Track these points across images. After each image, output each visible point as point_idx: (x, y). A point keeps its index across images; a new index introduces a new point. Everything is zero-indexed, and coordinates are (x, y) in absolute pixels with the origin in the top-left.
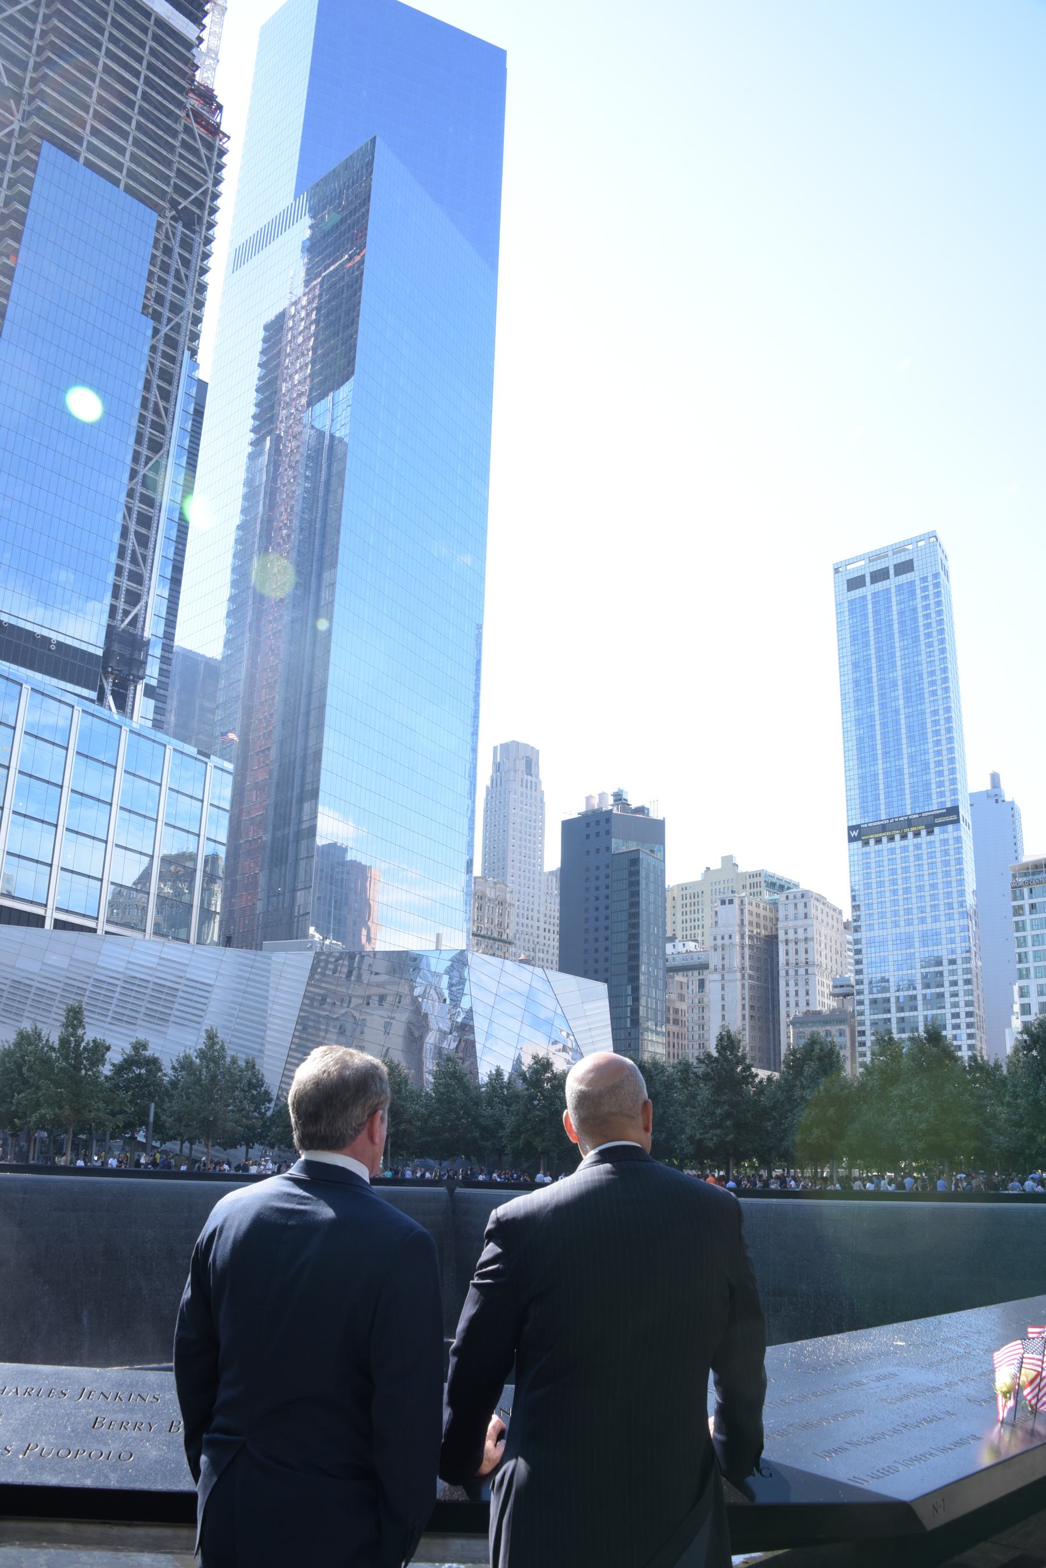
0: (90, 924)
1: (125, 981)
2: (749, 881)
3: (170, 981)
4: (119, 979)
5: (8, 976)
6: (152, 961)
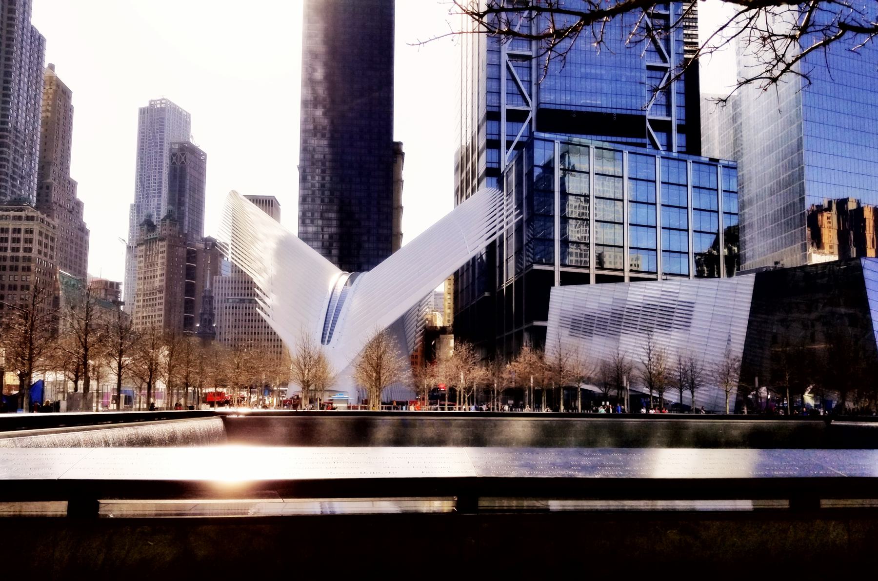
0: (654, 277)
3: (670, 304)
4: (640, 306)
5: (583, 312)
6: (657, 294)
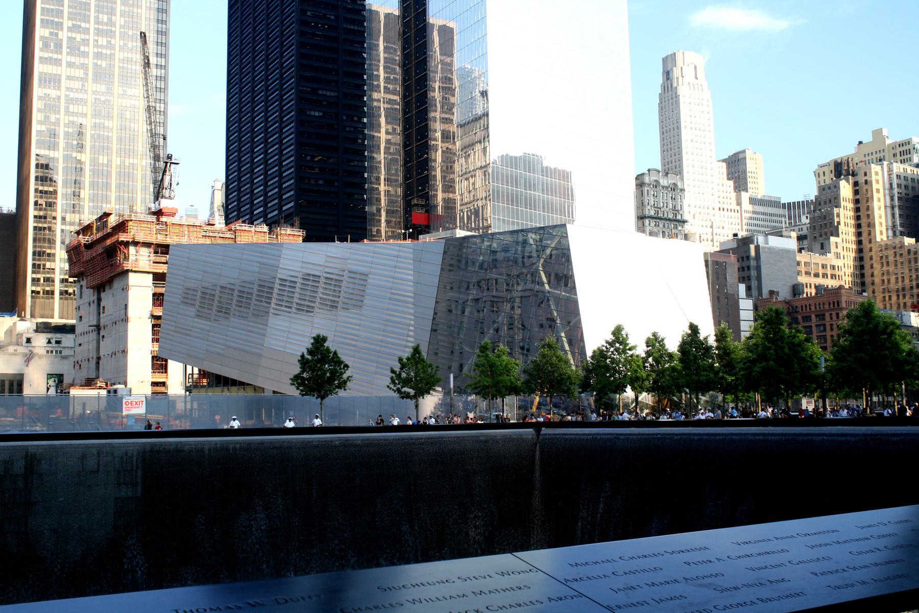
1: (303, 279)
2: (899, 150)
4: (297, 277)
6: (321, 260)
